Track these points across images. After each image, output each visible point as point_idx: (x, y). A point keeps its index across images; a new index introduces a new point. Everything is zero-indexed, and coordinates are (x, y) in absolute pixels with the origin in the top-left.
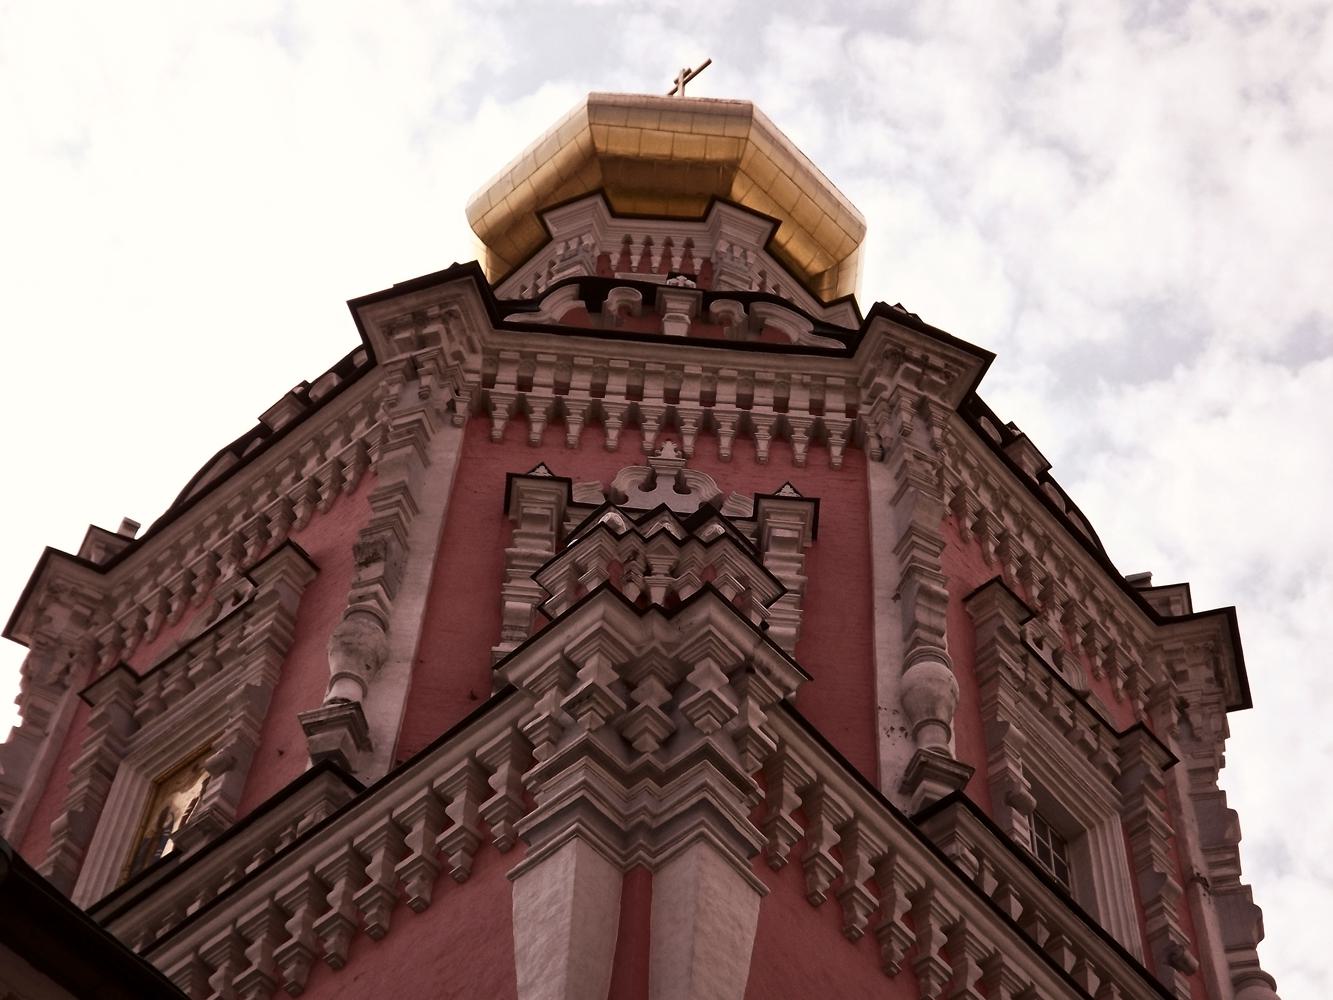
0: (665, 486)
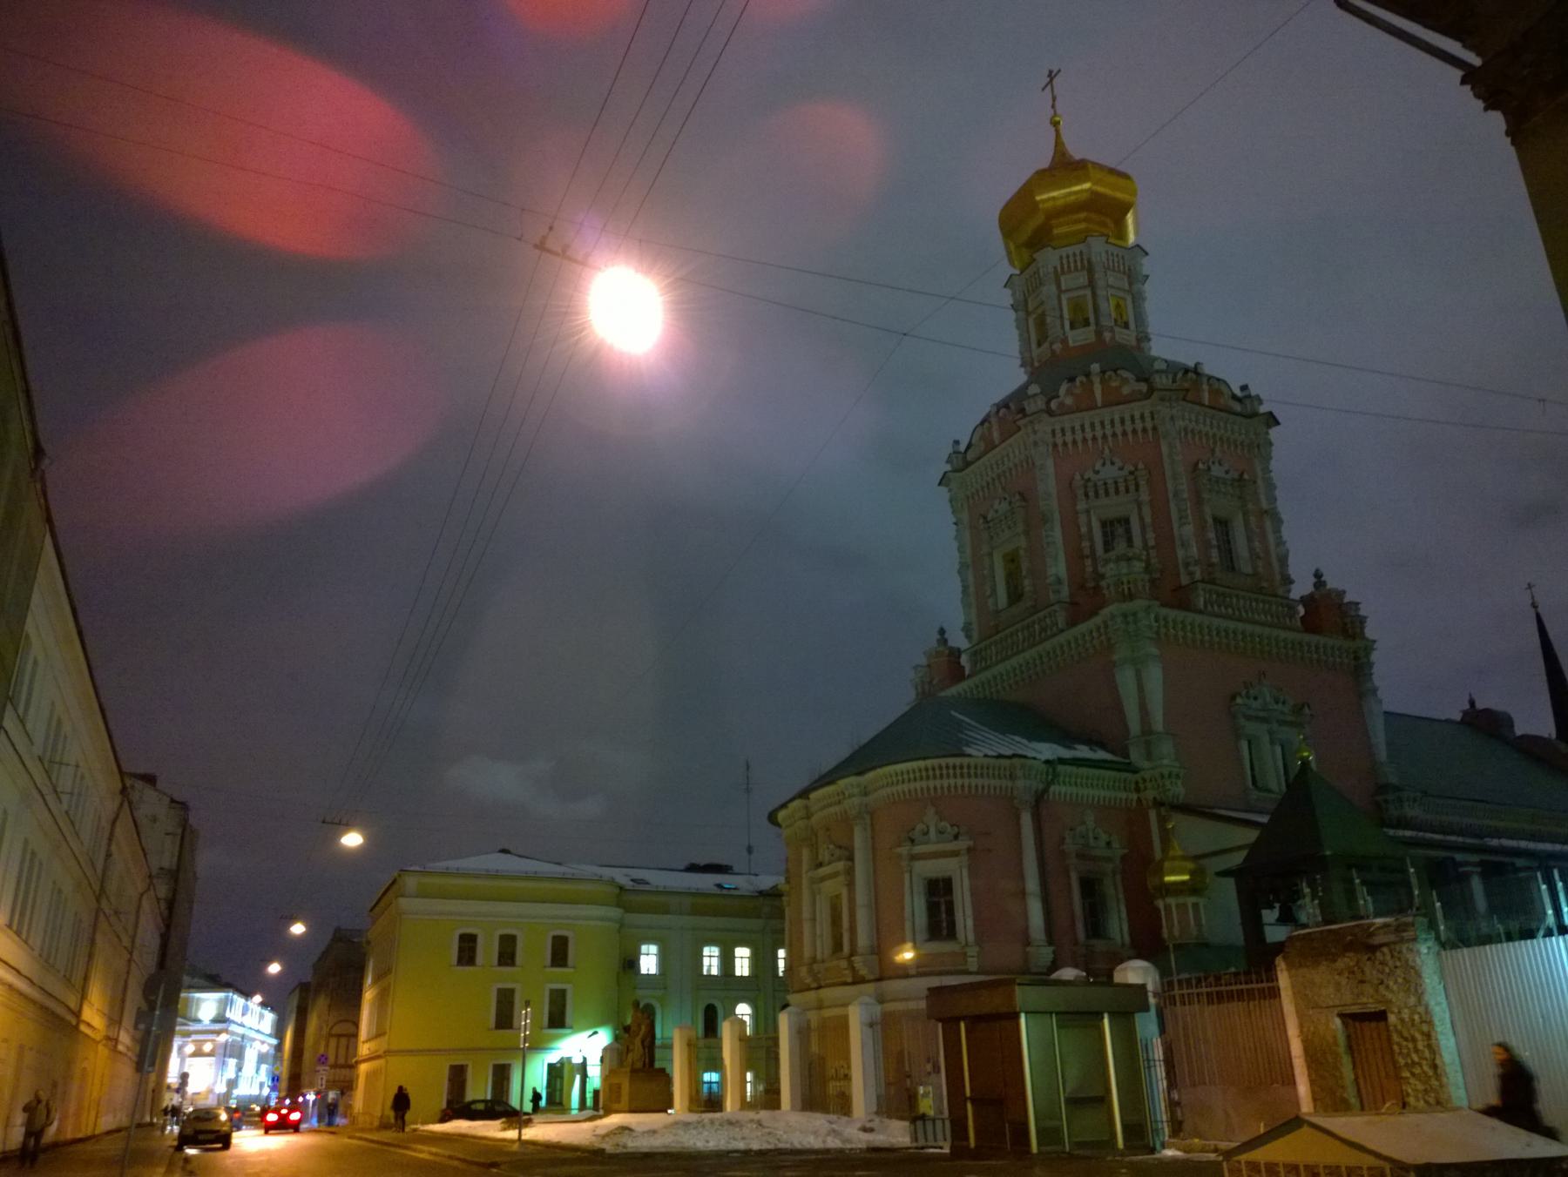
0: (1108, 463)
